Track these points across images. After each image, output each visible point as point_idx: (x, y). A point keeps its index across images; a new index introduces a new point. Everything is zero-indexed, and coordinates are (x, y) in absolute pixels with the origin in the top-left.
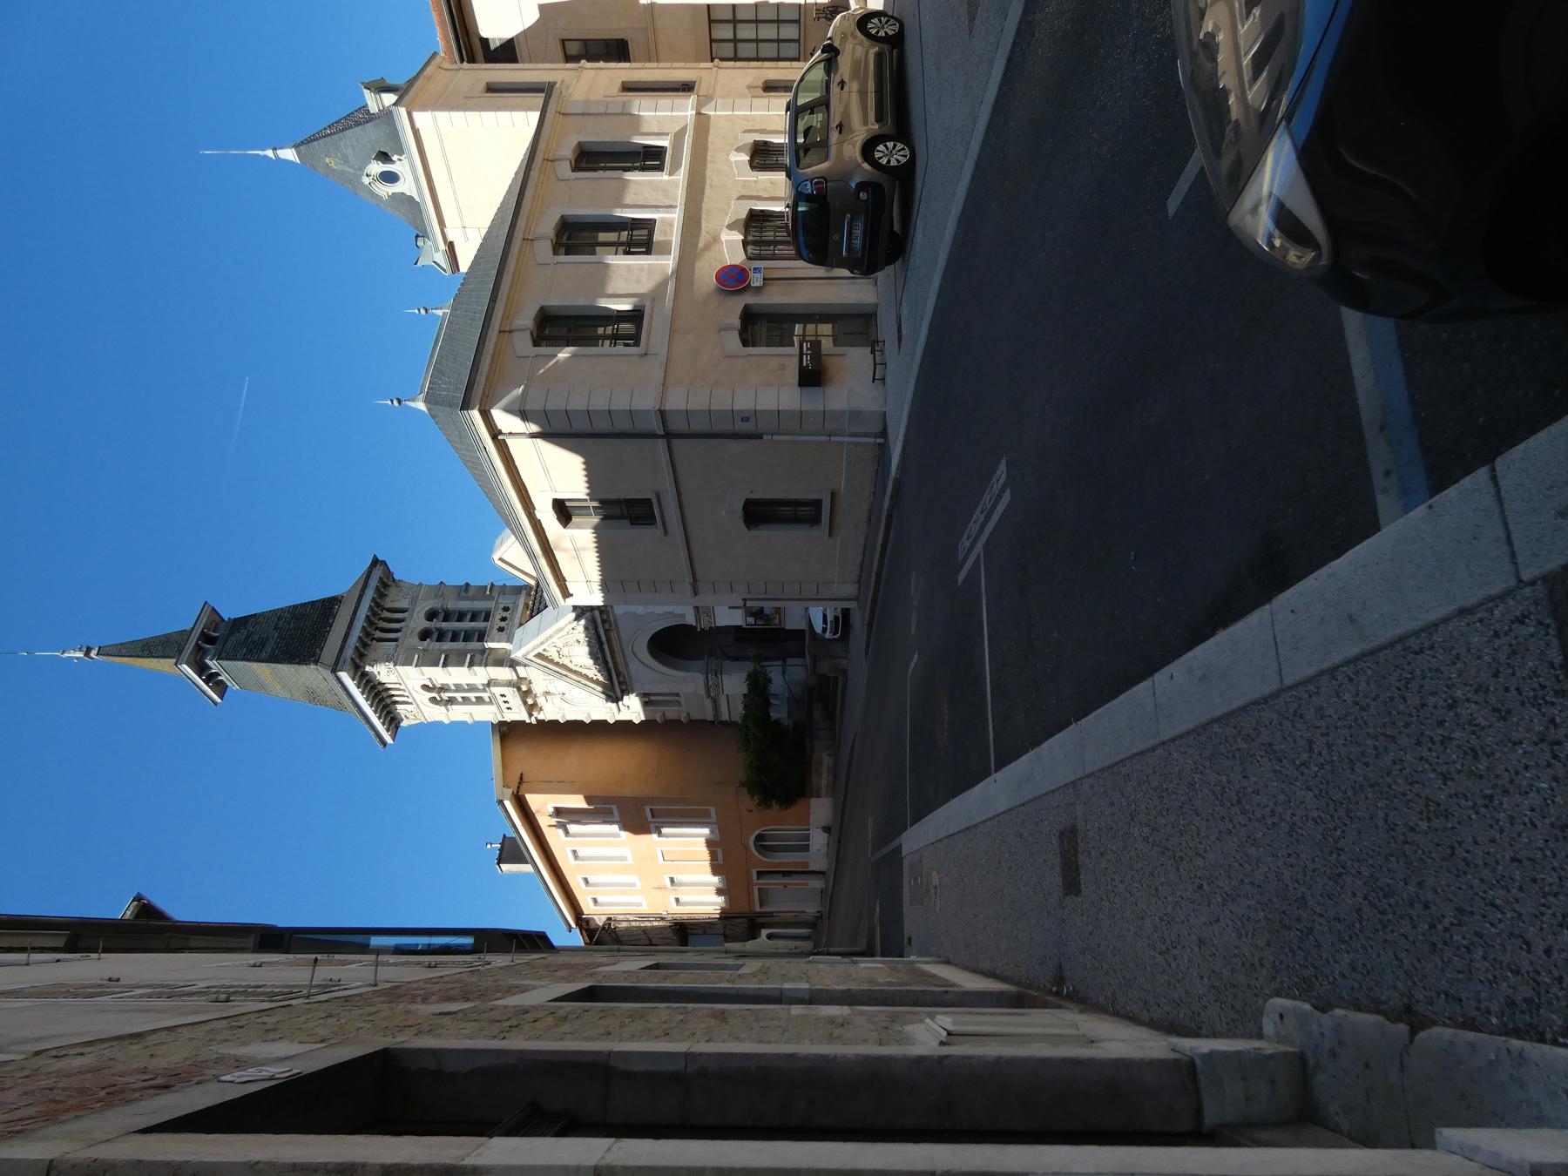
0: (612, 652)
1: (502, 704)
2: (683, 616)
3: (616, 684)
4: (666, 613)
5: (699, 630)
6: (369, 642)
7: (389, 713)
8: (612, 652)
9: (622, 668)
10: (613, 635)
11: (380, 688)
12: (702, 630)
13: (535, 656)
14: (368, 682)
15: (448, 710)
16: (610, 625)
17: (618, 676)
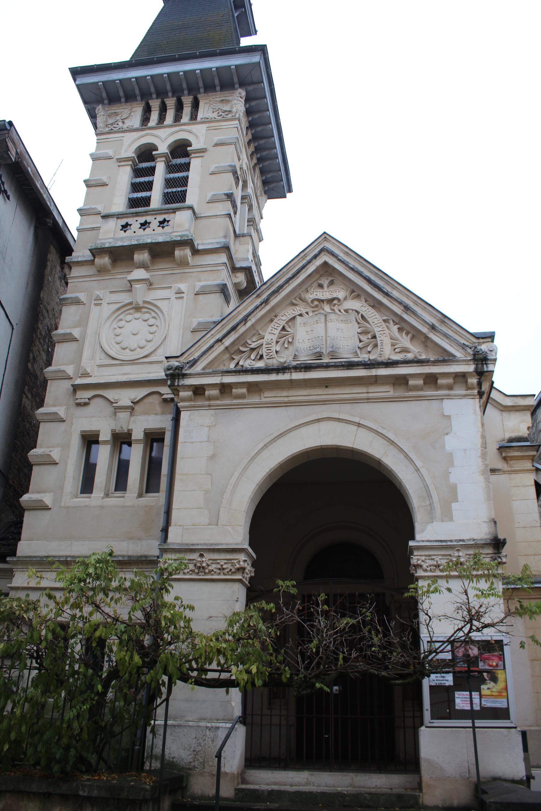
0: (326, 383)
1: (142, 220)
2: (448, 516)
3: (228, 379)
4: (453, 492)
5: (411, 543)
6: (250, 119)
7: (129, 98)
8: (326, 383)
9: (268, 396)
10: (388, 391)
11: (187, 101)
12: (411, 551)
13: (325, 264)
14: (209, 88)
15: (119, 160)
16: (416, 388)
17: (254, 388)
